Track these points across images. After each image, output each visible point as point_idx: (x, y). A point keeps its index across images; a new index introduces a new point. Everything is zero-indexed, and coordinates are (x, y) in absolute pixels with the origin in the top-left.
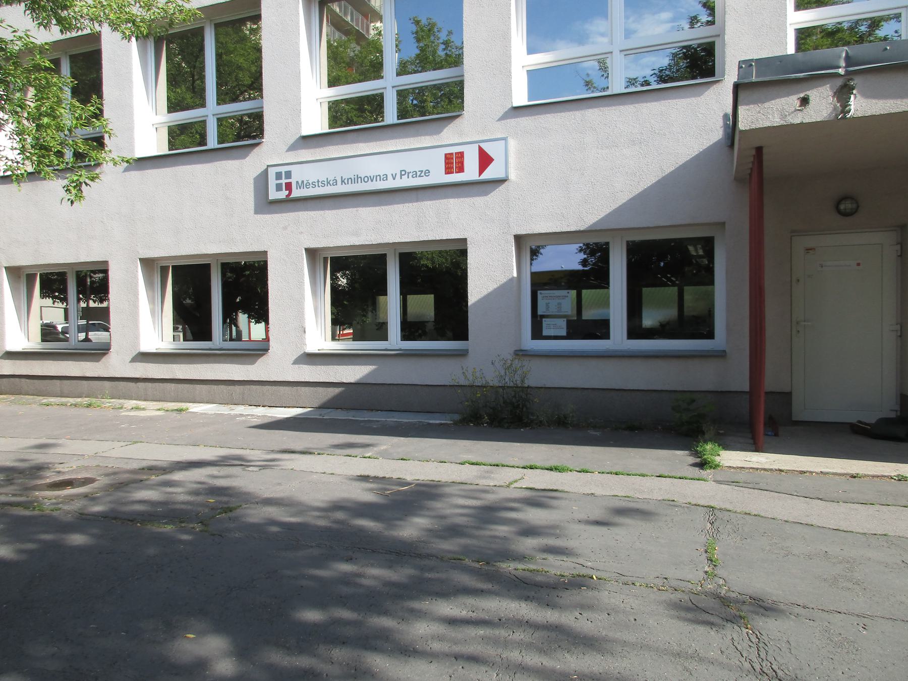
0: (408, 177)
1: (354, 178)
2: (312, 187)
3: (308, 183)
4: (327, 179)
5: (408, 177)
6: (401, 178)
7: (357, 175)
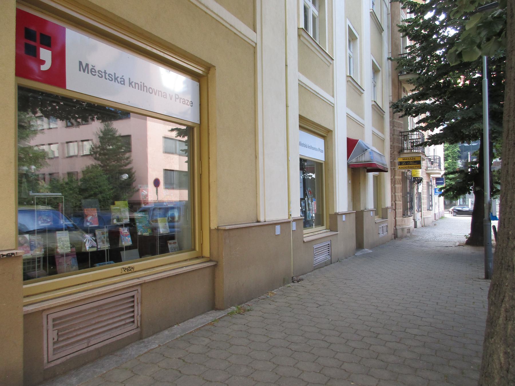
0: (180, 102)
2: (98, 75)
4: (115, 74)
5: (180, 102)
6: (176, 101)
7: (144, 83)
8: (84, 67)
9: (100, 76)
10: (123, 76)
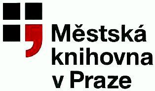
1: (82, 55)
2: (89, 39)
3: (81, 31)
4: (123, 27)
8: (61, 32)
9: (92, 38)
10: (141, 26)
